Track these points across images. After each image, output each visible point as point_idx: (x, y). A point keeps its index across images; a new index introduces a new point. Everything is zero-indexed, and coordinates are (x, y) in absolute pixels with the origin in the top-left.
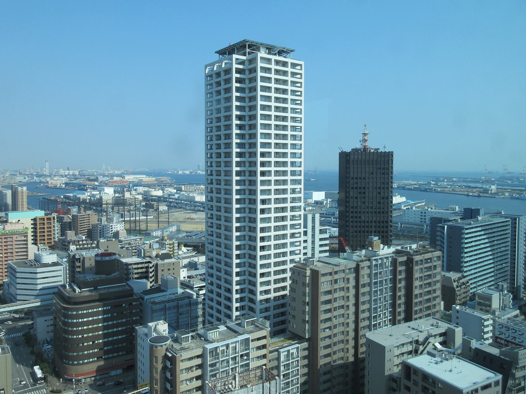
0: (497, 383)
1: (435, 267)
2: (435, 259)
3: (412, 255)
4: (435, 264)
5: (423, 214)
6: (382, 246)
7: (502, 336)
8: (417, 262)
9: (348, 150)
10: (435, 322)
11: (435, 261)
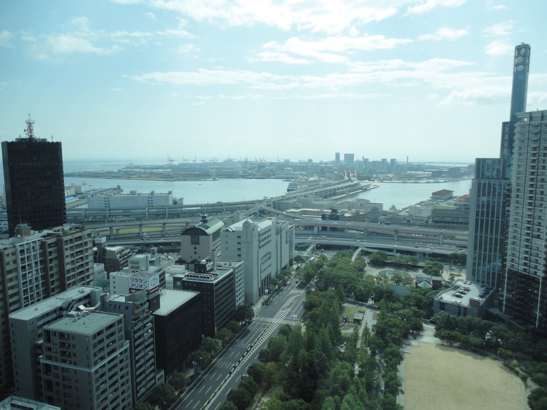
0: (120, 321)
1: (86, 243)
2: (86, 236)
3: (61, 236)
4: (85, 241)
5: (107, 200)
6: (32, 231)
7: (134, 287)
8: (66, 241)
9: (12, 139)
10: (81, 288)
11: (85, 239)
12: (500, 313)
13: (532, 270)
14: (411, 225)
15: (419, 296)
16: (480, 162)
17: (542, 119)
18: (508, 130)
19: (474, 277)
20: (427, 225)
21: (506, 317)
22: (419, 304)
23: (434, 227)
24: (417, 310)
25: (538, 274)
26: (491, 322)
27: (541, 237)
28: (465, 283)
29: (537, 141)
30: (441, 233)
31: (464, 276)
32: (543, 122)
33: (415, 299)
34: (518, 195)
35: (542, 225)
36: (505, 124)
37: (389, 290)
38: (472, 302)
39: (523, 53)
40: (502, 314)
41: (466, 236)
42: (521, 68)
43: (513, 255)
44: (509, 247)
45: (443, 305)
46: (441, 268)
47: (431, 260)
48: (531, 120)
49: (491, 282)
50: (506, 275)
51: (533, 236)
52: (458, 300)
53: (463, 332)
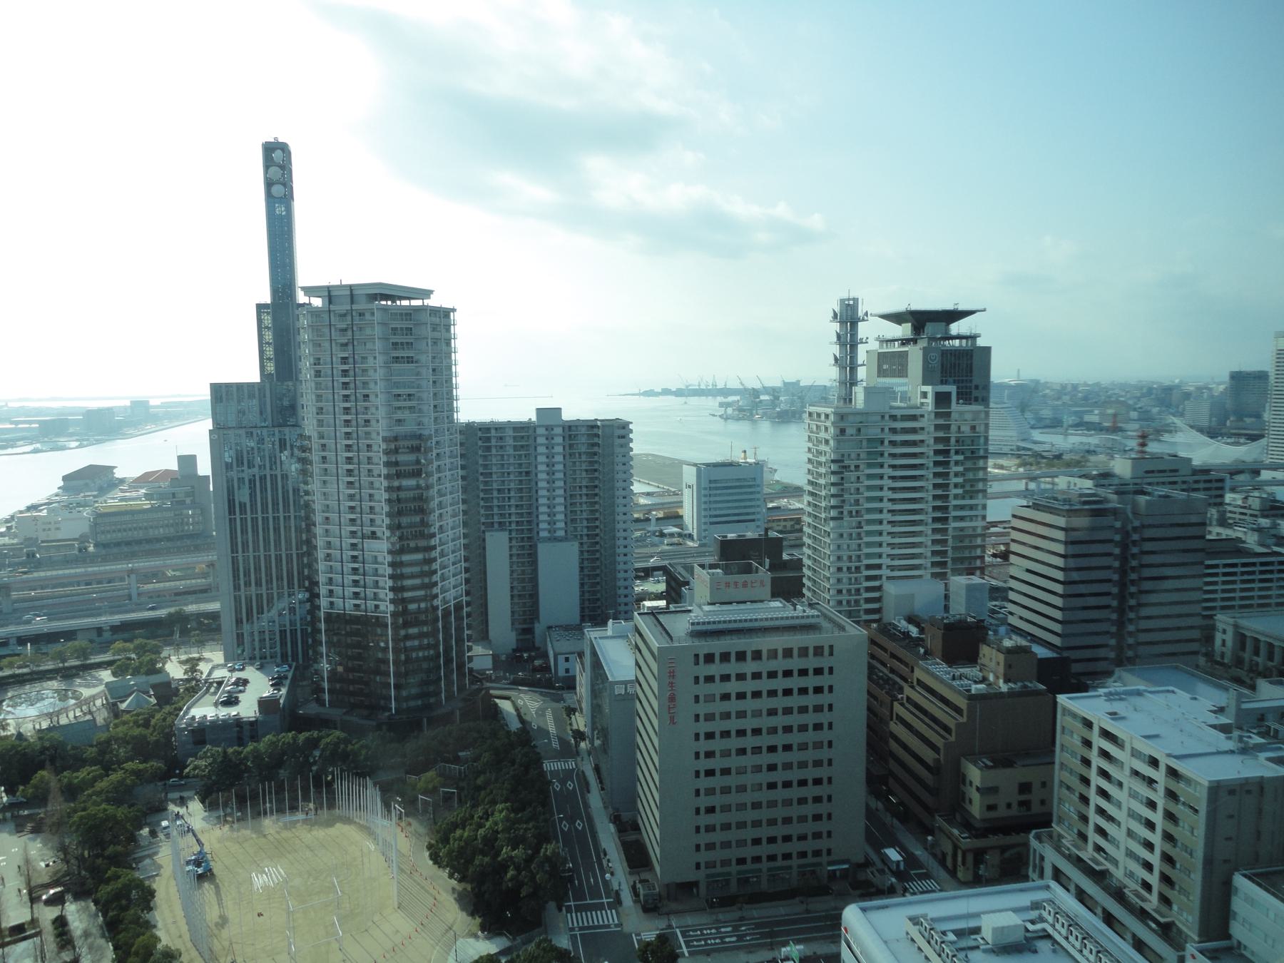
12: (321, 710)
13: (371, 604)
14: (39, 565)
15: (137, 731)
16: (221, 393)
17: (352, 302)
18: (280, 318)
19: (246, 651)
20: (83, 557)
21: (336, 714)
22: (141, 749)
23: (105, 560)
24: (141, 766)
25: (382, 608)
26: (315, 734)
27: (379, 534)
28: (232, 670)
29: (346, 345)
30: (131, 571)
31: (217, 656)
32: (354, 307)
33: (128, 743)
34: (324, 458)
35: (377, 510)
36: (260, 307)
37: (47, 744)
38: (264, 704)
39: (277, 159)
40: (327, 711)
41: (208, 562)
42: (277, 190)
43: (330, 581)
44: (321, 566)
45: (203, 733)
46: (157, 651)
47: (125, 641)
48: (330, 302)
49: (289, 651)
50: (323, 626)
51: (363, 537)
52: (233, 711)
53: (261, 773)
